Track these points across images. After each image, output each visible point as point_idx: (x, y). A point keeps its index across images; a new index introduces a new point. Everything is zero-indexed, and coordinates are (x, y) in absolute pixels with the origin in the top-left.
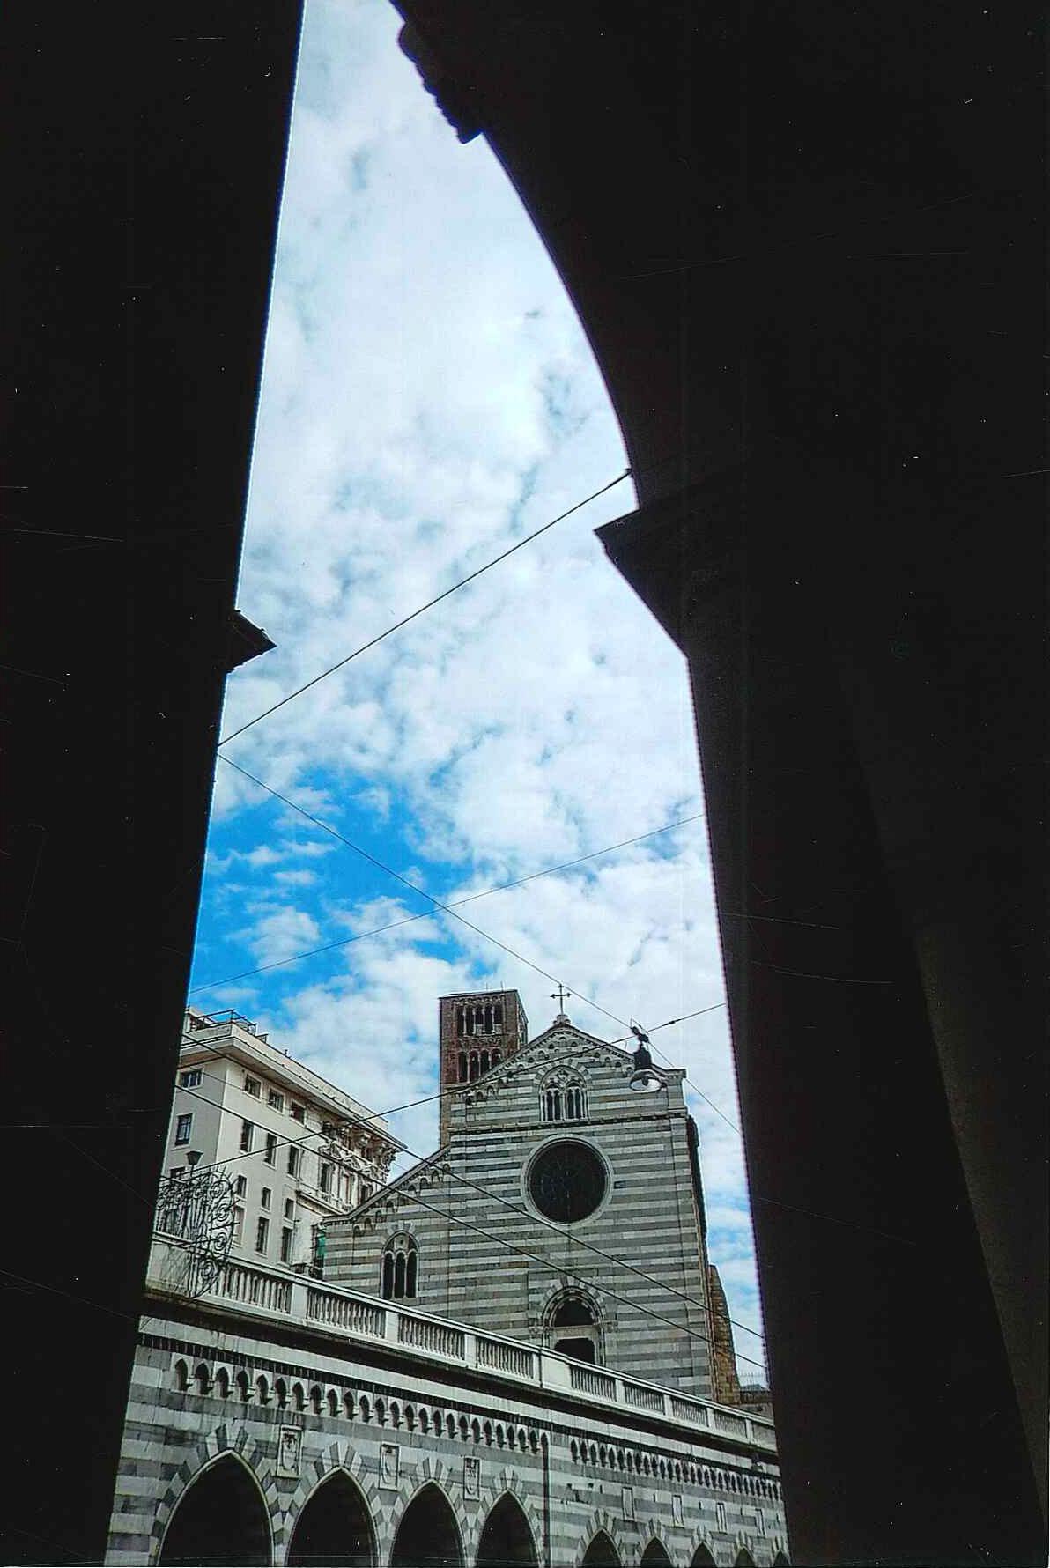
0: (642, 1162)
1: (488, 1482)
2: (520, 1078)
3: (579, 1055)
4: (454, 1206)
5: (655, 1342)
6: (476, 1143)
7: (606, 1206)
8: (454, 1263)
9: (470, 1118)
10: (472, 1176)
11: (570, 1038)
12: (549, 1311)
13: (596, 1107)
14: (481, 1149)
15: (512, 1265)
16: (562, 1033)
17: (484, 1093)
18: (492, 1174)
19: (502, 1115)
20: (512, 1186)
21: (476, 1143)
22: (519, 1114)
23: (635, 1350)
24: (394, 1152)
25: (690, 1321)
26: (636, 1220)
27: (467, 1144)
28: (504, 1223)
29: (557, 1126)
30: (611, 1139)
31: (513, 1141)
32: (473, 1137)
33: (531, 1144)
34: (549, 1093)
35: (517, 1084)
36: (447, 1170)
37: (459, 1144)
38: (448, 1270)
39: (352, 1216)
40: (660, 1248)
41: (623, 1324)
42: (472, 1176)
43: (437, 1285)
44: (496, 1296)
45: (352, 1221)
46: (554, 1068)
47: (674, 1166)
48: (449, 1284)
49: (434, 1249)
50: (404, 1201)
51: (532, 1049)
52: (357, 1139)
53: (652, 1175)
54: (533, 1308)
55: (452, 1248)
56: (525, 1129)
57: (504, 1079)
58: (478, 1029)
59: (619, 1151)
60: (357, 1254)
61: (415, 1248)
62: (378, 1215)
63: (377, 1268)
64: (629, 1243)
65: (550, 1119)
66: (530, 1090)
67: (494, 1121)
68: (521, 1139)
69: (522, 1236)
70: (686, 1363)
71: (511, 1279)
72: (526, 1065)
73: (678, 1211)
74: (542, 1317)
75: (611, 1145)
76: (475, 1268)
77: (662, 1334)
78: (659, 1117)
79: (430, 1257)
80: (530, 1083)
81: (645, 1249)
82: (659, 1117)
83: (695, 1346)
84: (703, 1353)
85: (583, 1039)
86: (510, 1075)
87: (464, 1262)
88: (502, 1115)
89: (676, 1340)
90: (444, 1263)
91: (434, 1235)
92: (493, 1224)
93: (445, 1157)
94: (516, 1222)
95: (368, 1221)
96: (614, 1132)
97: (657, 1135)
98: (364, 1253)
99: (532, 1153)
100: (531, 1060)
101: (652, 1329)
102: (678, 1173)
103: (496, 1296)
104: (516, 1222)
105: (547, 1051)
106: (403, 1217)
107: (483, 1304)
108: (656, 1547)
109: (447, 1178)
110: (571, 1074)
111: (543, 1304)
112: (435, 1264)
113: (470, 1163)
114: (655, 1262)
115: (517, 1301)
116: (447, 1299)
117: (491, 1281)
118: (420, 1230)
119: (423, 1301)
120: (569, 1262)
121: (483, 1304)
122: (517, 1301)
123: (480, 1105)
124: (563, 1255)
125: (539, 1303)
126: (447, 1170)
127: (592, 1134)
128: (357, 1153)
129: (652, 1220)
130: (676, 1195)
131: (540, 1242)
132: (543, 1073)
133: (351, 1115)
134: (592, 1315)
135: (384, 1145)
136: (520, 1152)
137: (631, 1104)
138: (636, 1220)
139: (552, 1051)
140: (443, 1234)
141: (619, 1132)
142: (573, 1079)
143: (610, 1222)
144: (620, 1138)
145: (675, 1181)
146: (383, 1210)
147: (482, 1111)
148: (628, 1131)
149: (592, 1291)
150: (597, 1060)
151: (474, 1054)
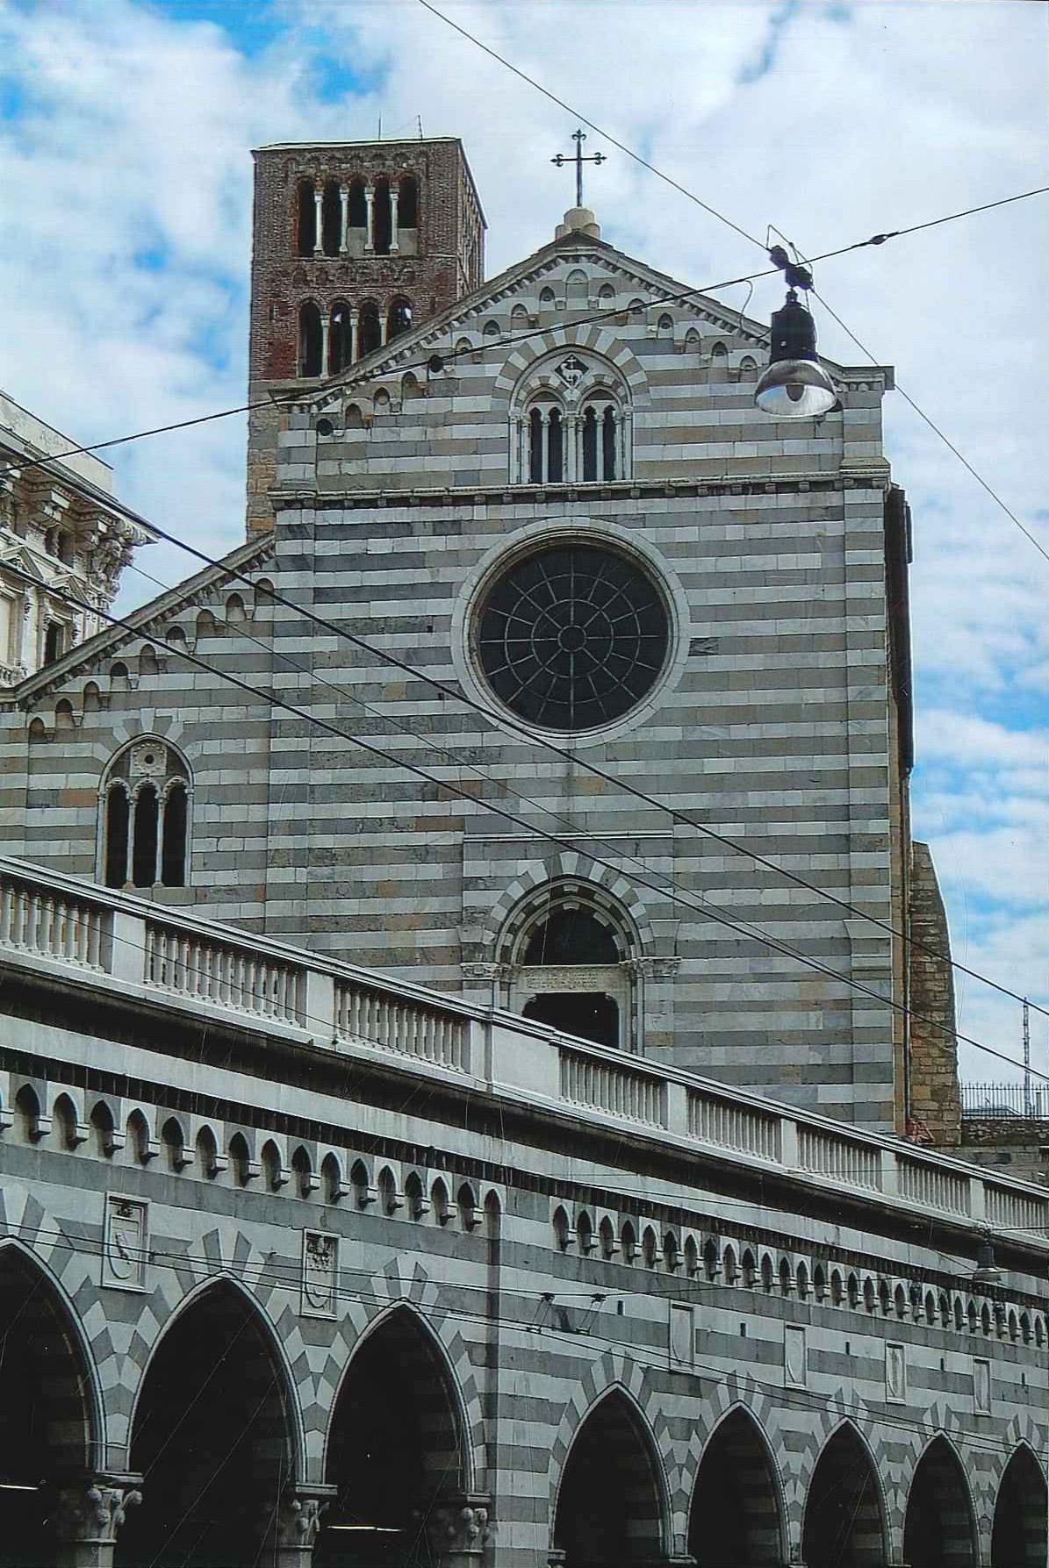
0: (763, 594)
1: (356, 1285)
2: (463, 371)
3: (619, 318)
4: (281, 681)
5: (765, 1007)
6: (343, 532)
7: (665, 694)
8: (281, 812)
9: (329, 468)
10: (326, 612)
11: (596, 272)
12: (513, 930)
13: (653, 453)
14: (353, 546)
15: (424, 824)
16: (576, 259)
17: (367, 407)
18: (380, 609)
19: (408, 465)
20: (430, 640)
21: (343, 532)
23: (715, 1023)
24: (129, 544)
25: (855, 965)
26: (740, 732)
27: (319, 532)
28: (406, 725)
29: (551, 497)
30: (690, 534)
31: (439, 528)
32: (334, 517)
33: (480, 541)
34: (535, 414)
35: (452, 388)
36: (264, 592)
37: (296, 531)
38: (267, 829)
39: (24, 692)
40: (795, 798)
41: (691, 966)
42: (326, 612)
43: (237, 861)
44: (383, 890)
45: (25, 706)
46: (553, 351)
47: (844, 608)
48: (268, 859)
49: (228, 777)
50: (153, 663)
51: (495, 299)
52: (34, 508)
53: (789, 627)
54: (473, 921)
55: (277, 777)
56: (469, 500)
57: (421, 374)
58: (356, 242)
59: (708, 564)
60: (40, 781)
61: (184, 773)
62: (90, 692)
63: (97, 816)
64: (718, 783)
65: (536, 476)
66: (484, 403)
67: (395, 479)
68: (456, 527)
69: (451, 757)
70: (839, 1054)
71: (422, 854)
72: (478, 340)
73: (845, 712)
74: (495, 942)
75: (688, 550)
76: (330, 826)
77: (788, 990)
78: (816, 486)
79: (221, 795)
80: (489, 387)
81: (755, 799)
82: (816, 486)
83: (861, 1018)
84: (877, 1034)
85: (633, 276)
87: (303, 811)
88: (408, 465)
89: (818, 1004)
90: (257, 813)
91: (230, 747)
92: (382, 725)
93: (261, 562)
94: (440, 724)
95: (64, 707)
96: (695, 519)
97: (806, 530)
98: (58, 781)
99: (487, 560)
100: (491, 327)
101: (761, 978)
102: (855, 624)
103: (383, 890)
104: (440, 724)
105: (533, 305)
106: (153, 699)
107: (351, 907)
108: (739, 1429)
109: (264, 613)
110: (596, 368)
111: (500, 914)
112: (233, 813)
113: (326, 580)
114: (778, 829)
115: (433, 905)
116: (262, 893)
117: (372, 855)
118: (195, 732)
119: (201, 896)
120: (566, 820)
121: (351, 907)
122: (433, 905)
123: (355, 435)
124: (552, 804)
125: (486, 911)
126: (264, 592)
127: (642, 520)
128: (34, 542)
129: (779, 731)
130: (844, 676)
131: (498, 772)
132: (520, 362)
133: (19, 448)
134: (618, 941)
135: (102, 527)
136: (454, 558)
137: (746, 450)
138: (740, 732)
139: (549, 306)
140: (253, 746)
141: (710, 519)
142: (600, 383)
143: (673, 734)
144: (712, 533)
145: (844, 642)
146: (103, 682)
147: (360, 451)
148: (735, 516)
149: (620, 888)
150: (664, 333)
151: (341, 307)
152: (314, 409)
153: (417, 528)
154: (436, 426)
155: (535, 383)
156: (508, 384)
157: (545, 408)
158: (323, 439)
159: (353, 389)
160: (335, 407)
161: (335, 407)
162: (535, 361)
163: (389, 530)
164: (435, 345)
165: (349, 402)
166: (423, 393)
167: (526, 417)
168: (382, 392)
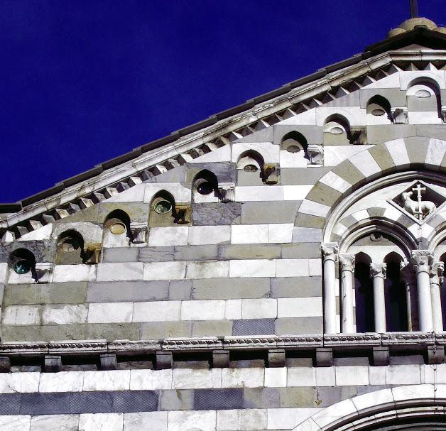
2: (246, 192)
16: (422, 66)
17: (92, 234)
22: (233, 309)
29: (399, 354)
35: (232, 212)
46: (390, 174)
56: (258, 357)
57: (182, 195)
66: (283, 232)
72: (274, 154)
86: (207, 181)
123: (70, 273)
147: (79, 294)
152: (9, 237)
153: (164, 401)
154: (202, 260)
155: (360, 213)
156: (321, 210)
157: (378, 254)
158: (15, 278)
159: (71, 211)
160: (41, 233)
161: (41, 233)
162: (361, 185)
163: (119, 401)
164: (204, 158)
165: (63, 228)
166: (180, 217)
167: (348, 254)
168: (120, 216)
